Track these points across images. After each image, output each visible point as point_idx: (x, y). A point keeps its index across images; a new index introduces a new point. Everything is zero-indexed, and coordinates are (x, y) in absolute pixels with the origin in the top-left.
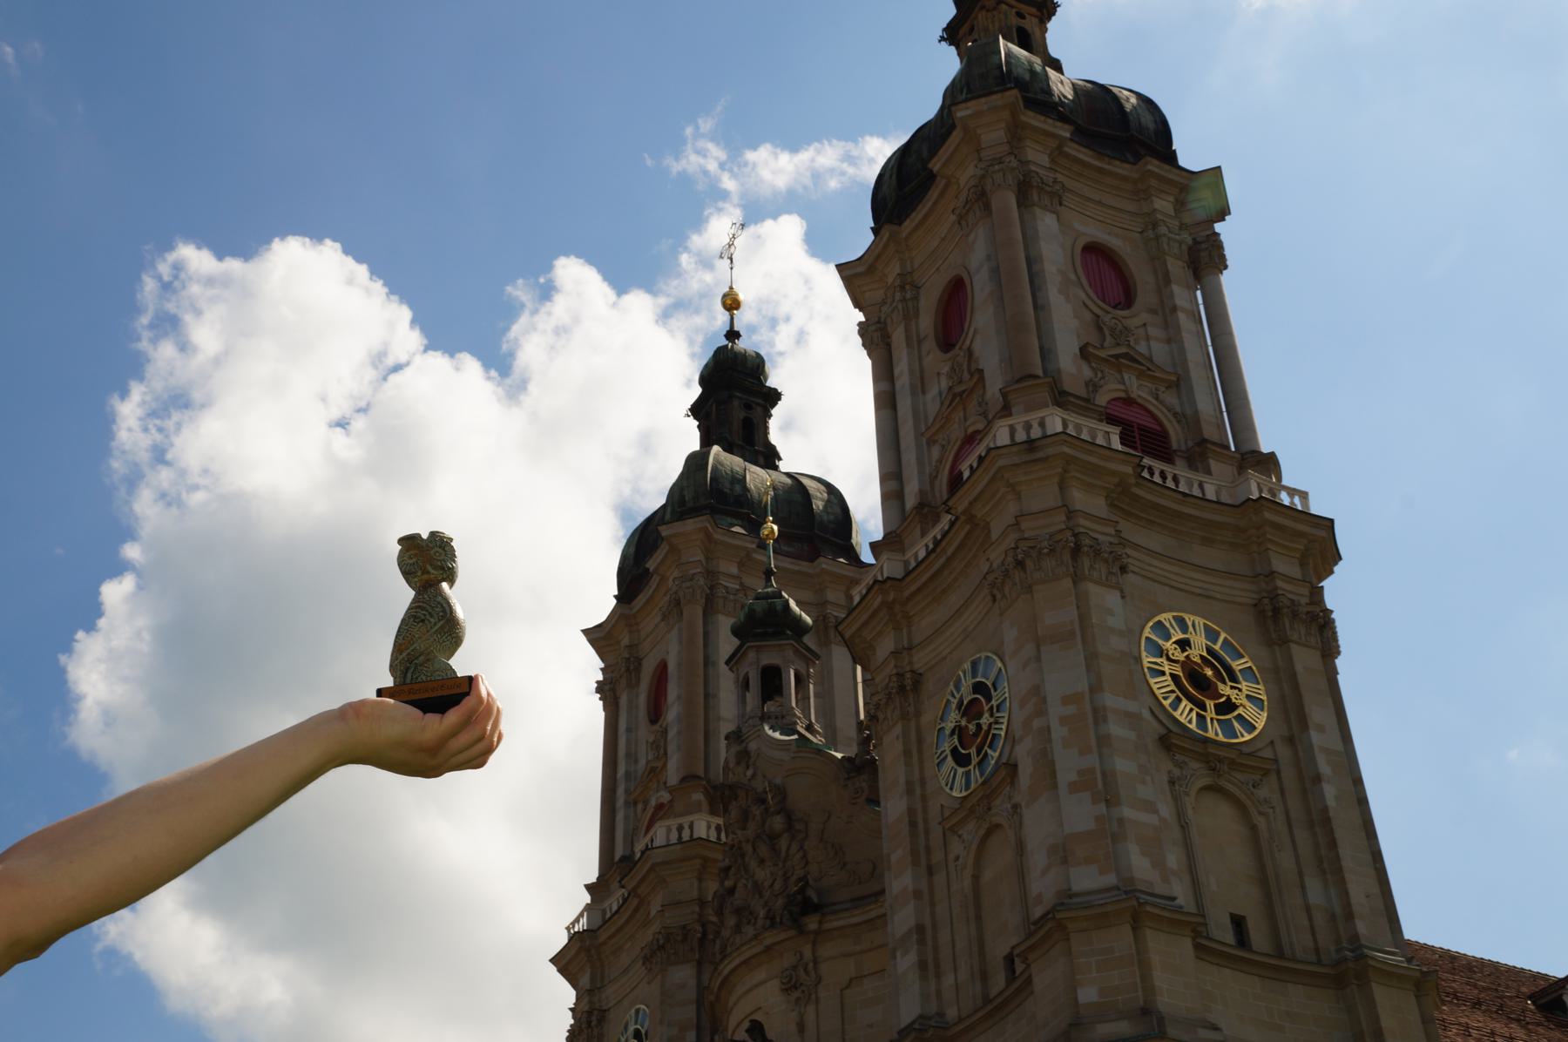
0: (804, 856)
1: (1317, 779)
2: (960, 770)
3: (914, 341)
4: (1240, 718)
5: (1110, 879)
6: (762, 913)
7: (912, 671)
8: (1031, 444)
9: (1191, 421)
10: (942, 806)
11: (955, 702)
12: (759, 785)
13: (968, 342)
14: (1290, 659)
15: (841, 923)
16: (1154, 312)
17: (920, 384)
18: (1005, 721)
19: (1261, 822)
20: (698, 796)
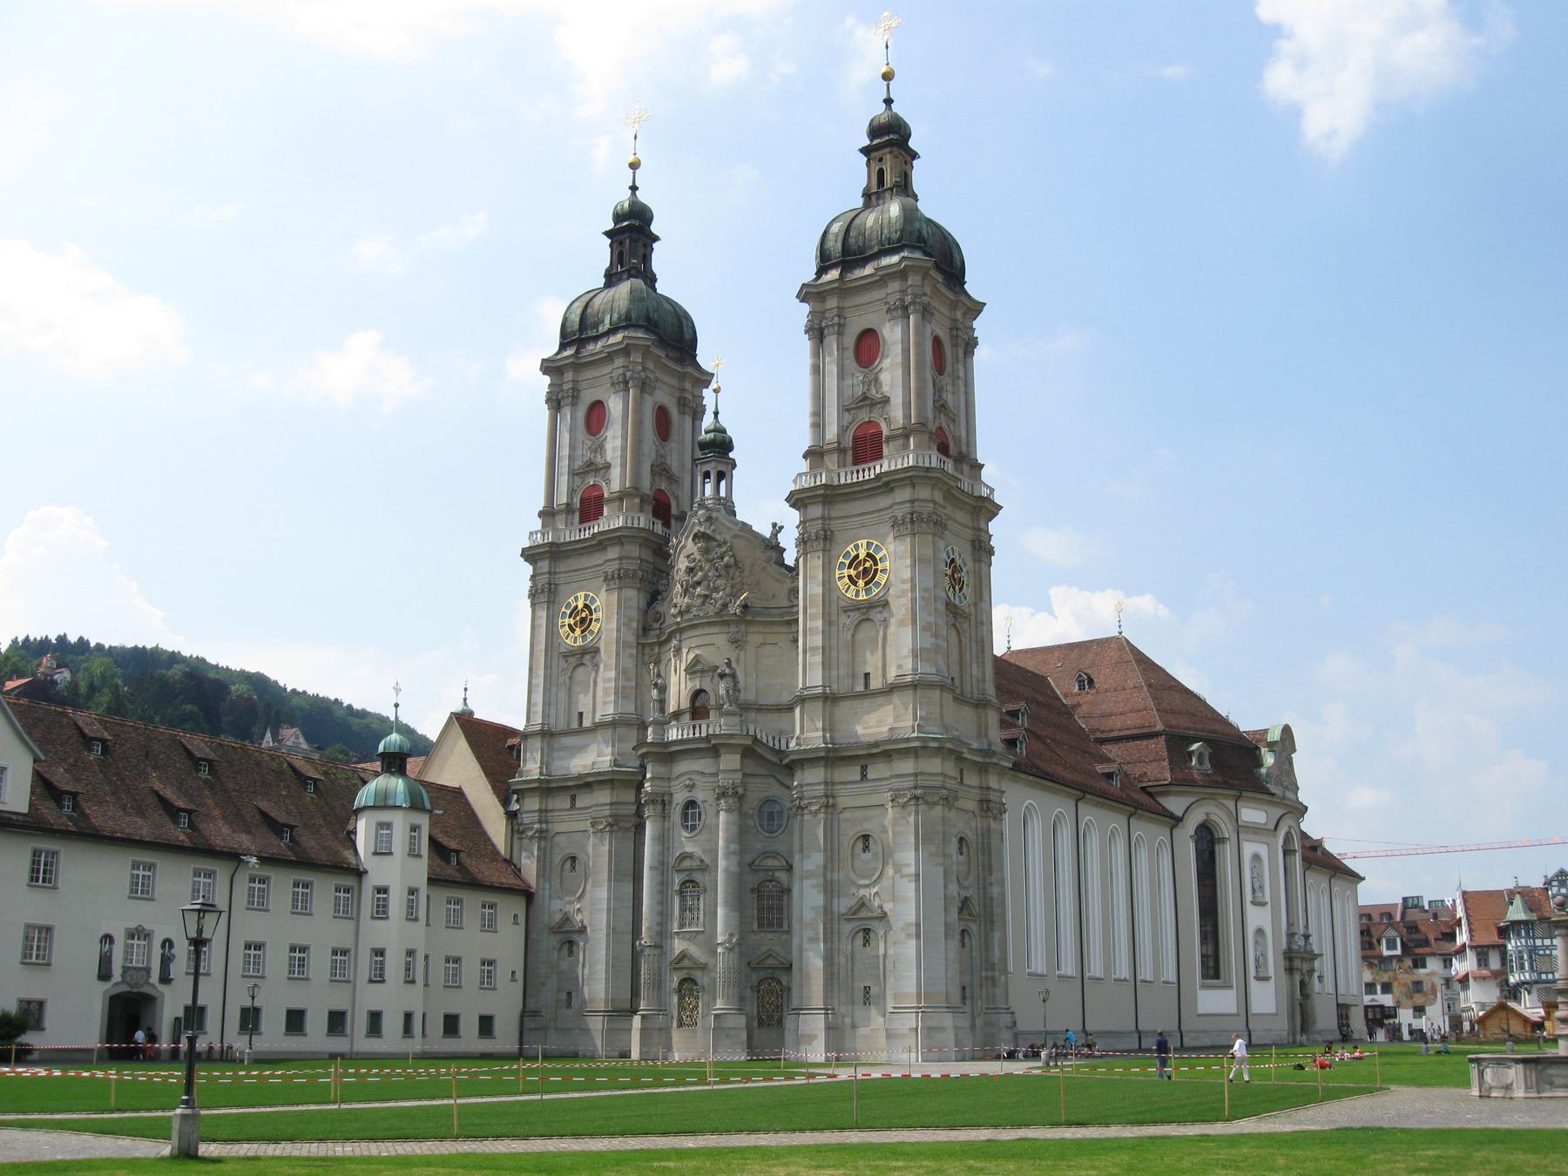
0: (741, 581)
1: (982, 623)
2: (853, 587)
3: (841, 349)
4: (963, 594)
5: (933, 670)
6: (720, 602)
7: (829, 529)
8: (927, 470)
9: (958, 440)
10: (838, 597)
11: (853, 554)
12: (718, 537)
13: (876, 371)
14: (980, 569)
15: (760, 619)
16: (949, 376)
17: (842, 375)
18: (885, 579)
19: (963, 639)
20: (637, 500)
